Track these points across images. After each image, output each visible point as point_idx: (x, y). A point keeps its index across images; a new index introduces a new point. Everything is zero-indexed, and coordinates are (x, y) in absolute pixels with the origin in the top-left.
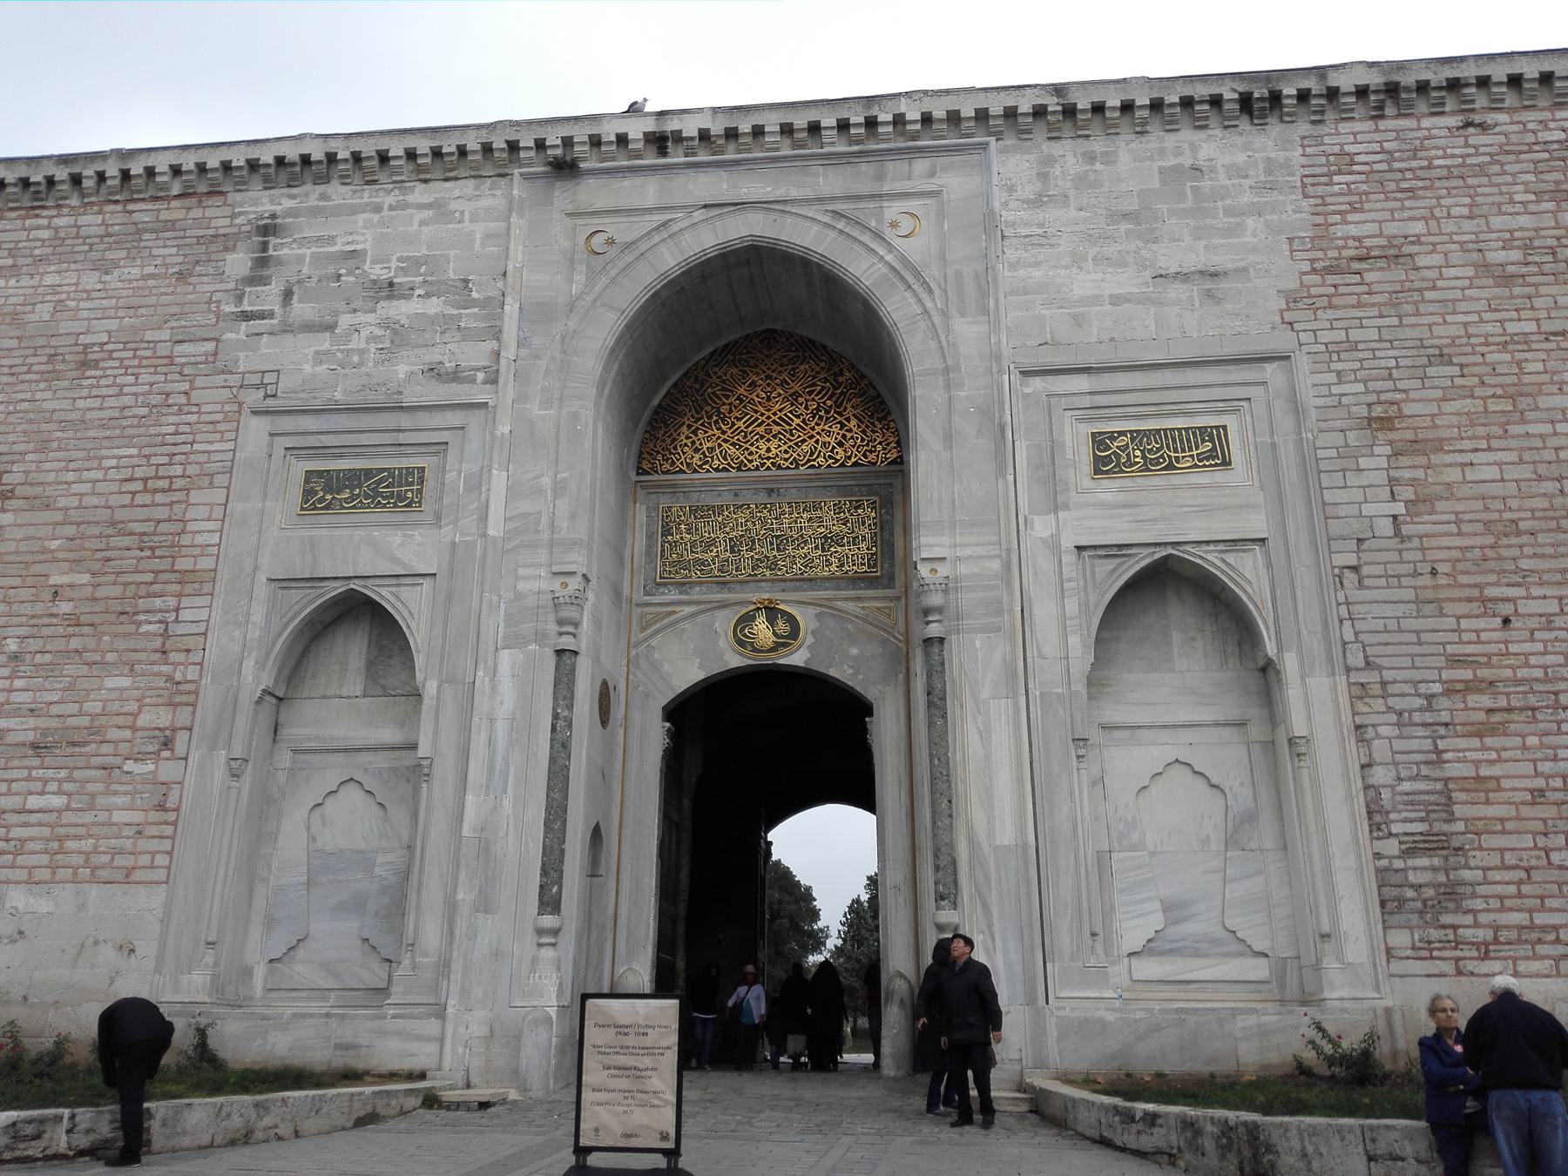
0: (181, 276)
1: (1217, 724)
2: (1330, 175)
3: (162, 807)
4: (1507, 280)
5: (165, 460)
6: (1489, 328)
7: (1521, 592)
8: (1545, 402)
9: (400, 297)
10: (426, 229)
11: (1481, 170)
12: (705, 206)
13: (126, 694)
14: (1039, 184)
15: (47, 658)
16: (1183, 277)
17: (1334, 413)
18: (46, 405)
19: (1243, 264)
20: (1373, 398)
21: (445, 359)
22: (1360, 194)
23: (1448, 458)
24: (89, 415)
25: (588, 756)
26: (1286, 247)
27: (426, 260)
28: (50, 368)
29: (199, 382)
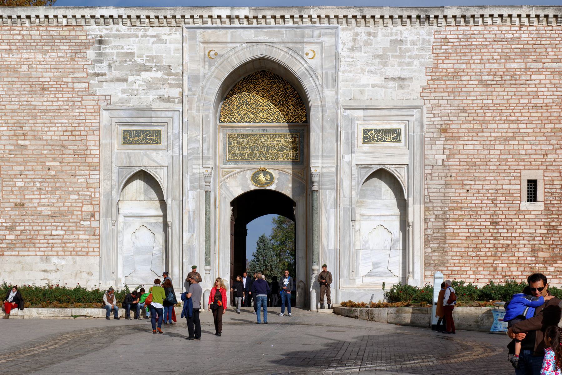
0: (72, 59)
1: (392, 215)
2: (441, 46)
3: (94, 235)
4: (486, 86)
5: (77, 125)
6: (479, 102)
7: (473, 183)
8: (490, 126)
9: (148, 71)
10: (155, 46)
13: (78, 201)
14: (353, 43)
15: (50, 189)
16: (393, 79)
17: (431, 127)
18: (33, 103)
19: (412, 76)
20: (442, 122)
22: (449, 53)
26: (425, 71)
28: (31, 89)
29: (84, 97)
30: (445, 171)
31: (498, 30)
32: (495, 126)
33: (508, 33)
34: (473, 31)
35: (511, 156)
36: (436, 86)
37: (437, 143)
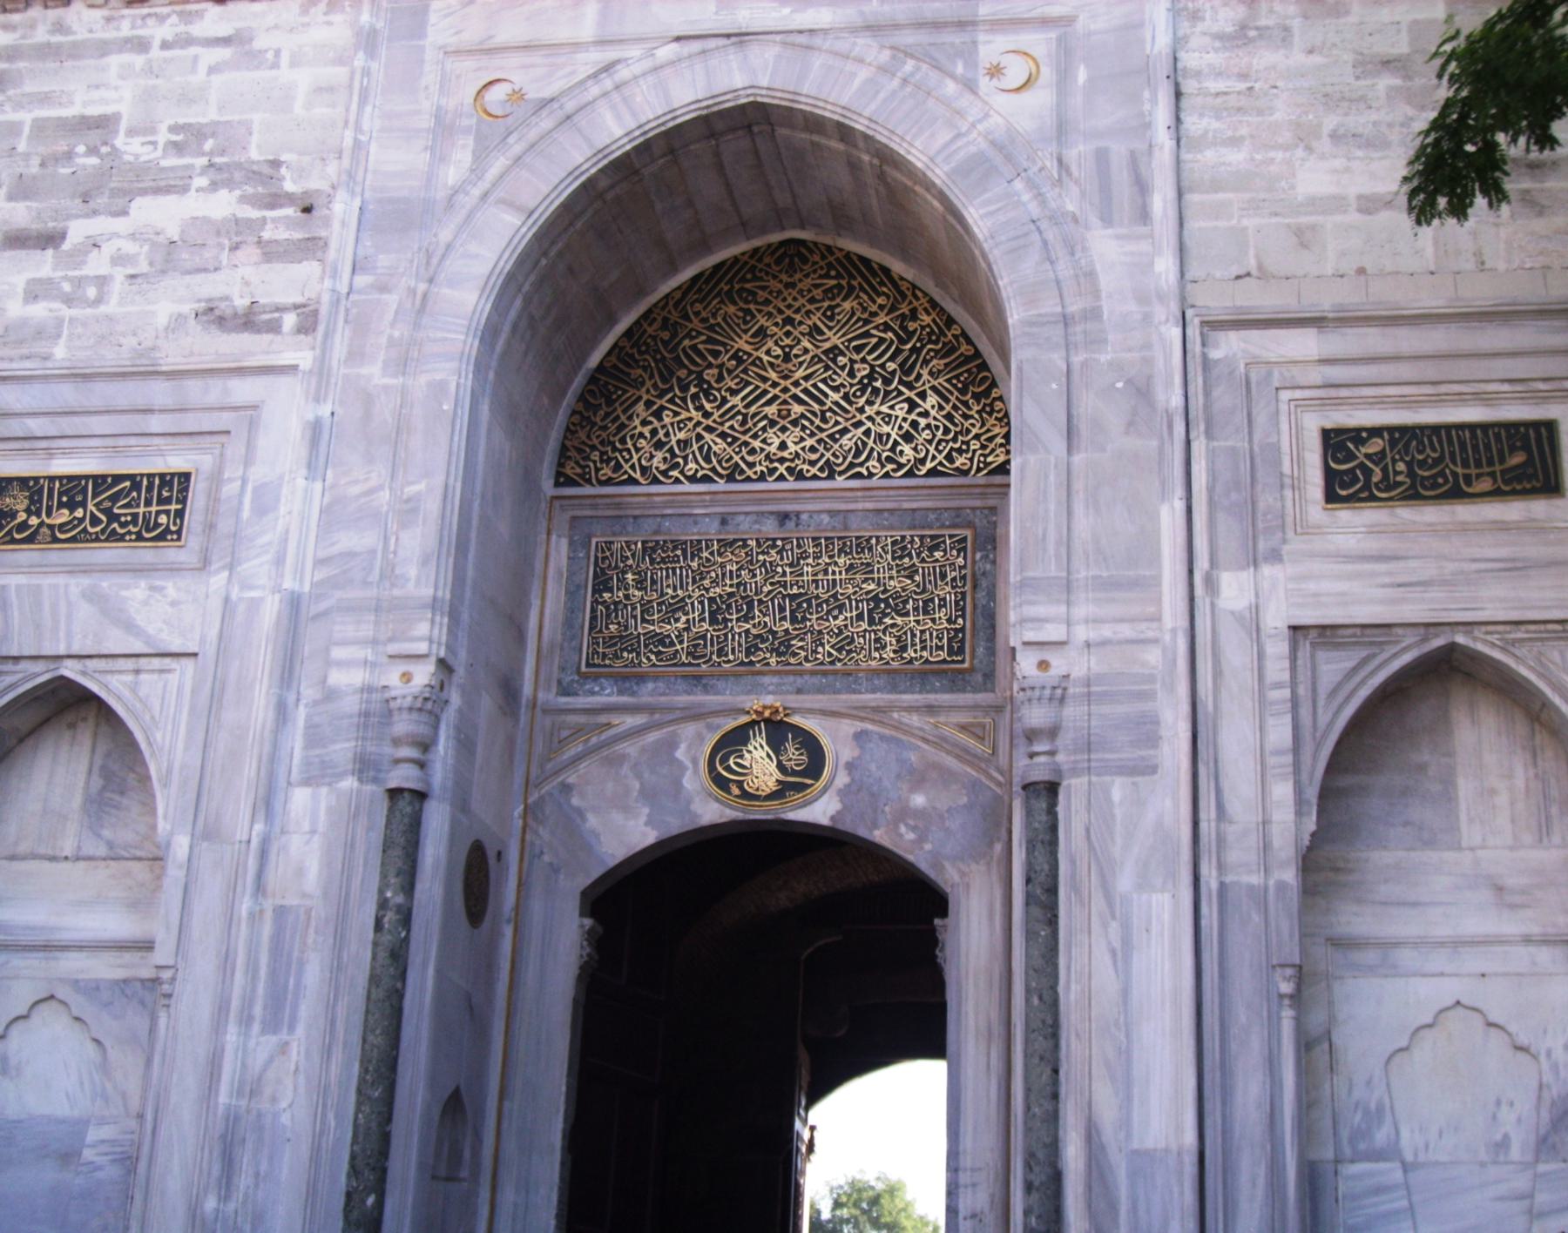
1: (1527, 940)
10: (217, 79)
12: (678, 39)
25: (439, 972)
27: (211, 130)
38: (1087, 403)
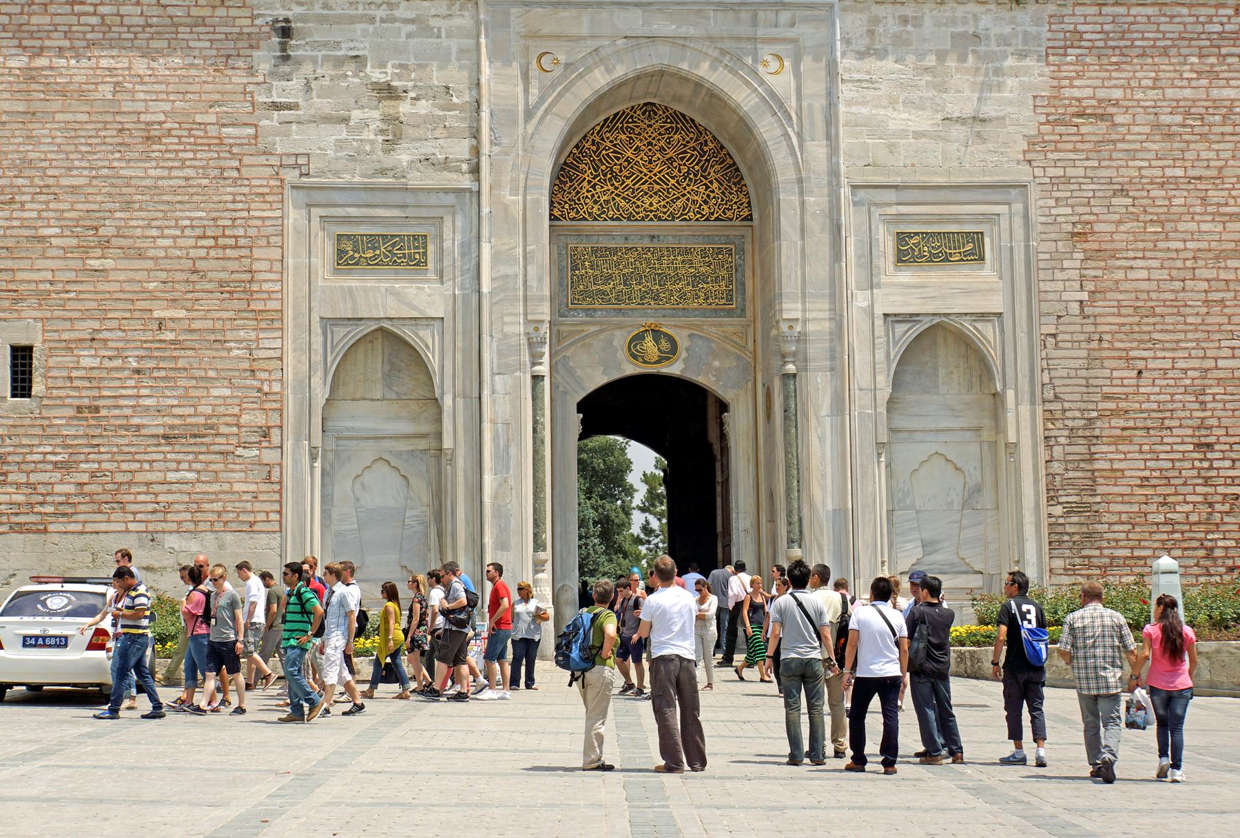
2: (1066, 48)
3: (268, 479)
5: (229, 223)
8: (1182, 226)
10: (413, 41)
11: (1165, 52)
13: (229, 401)
16: (961, 120)
17: (1051, 228)
19: (1002, 114)
21: (436, 151)
23: (1119, 263)
24: (160, 183)
26: (1031, 102)
29: (246, 160)
30: (1086, 328)
31: (1190, 15)
32: (1192, 226)
33: (1211, 22)
34: (1135, 16)
35: (1231, 295)
36: (1058, 138)
37: (1066, 264)
38: (809, 219)
